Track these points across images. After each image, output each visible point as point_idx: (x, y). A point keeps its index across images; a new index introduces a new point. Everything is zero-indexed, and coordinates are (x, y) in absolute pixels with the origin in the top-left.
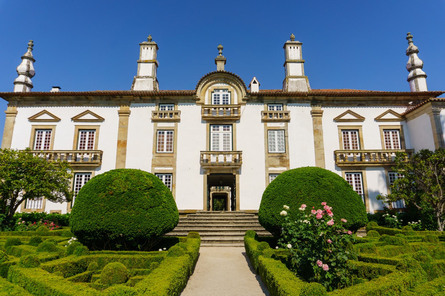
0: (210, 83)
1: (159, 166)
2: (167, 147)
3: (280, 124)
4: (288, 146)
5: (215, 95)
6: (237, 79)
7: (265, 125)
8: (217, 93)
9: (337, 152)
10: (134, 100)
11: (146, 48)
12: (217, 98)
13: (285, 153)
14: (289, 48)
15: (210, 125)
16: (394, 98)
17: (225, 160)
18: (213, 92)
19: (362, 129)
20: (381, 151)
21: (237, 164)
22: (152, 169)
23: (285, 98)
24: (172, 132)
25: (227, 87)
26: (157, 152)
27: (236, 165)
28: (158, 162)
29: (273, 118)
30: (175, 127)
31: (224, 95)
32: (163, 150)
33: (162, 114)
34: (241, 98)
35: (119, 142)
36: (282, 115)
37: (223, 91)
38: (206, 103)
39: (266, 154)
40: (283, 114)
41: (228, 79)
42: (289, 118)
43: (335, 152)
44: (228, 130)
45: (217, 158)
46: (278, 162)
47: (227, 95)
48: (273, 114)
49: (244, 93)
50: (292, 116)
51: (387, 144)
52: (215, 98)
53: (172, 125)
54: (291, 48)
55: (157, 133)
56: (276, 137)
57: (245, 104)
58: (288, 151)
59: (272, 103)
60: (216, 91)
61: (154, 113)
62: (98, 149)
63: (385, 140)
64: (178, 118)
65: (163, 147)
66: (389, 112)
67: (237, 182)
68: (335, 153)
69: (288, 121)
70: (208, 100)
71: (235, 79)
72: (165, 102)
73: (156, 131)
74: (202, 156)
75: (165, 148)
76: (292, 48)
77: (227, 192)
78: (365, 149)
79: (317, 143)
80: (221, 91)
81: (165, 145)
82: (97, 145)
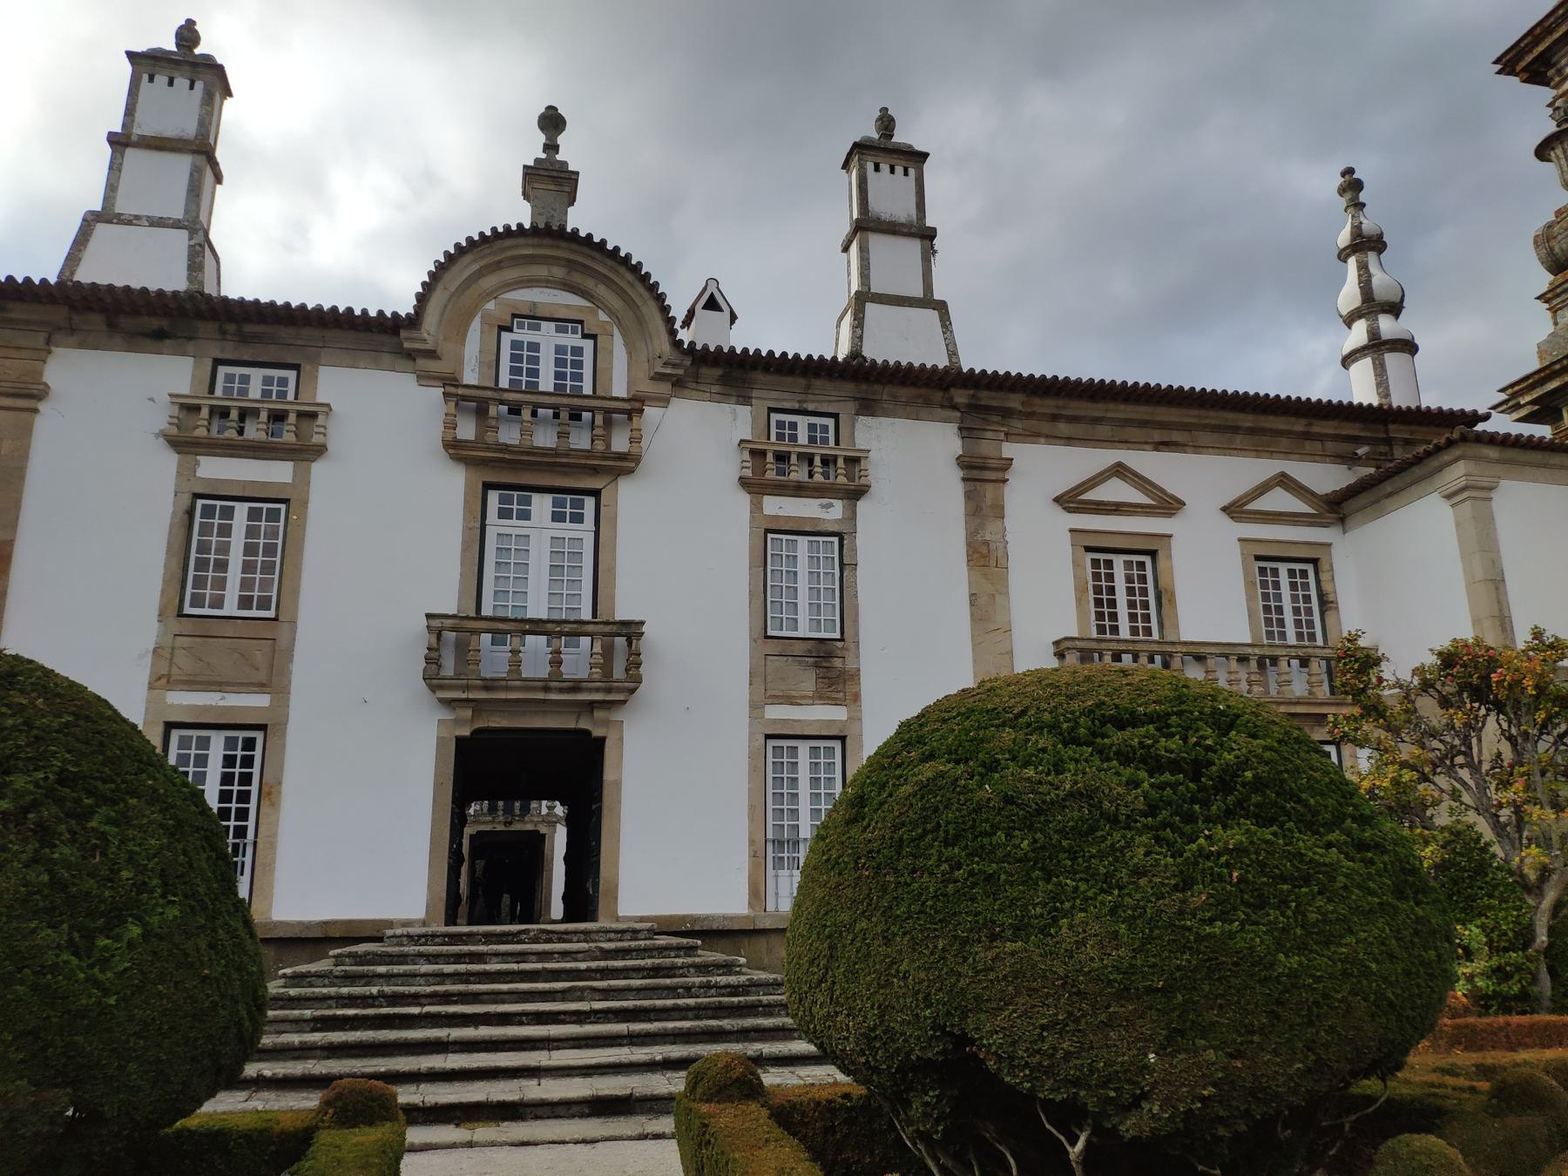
0: (489, 282)
1: (192, 684)
2: (246, 584)
5: (516, 345)
6: (629, 276)
7: (757, 507)
9: (1063, 646)
12: (525, 357)
13: (842, 640)
14: (870, 166)
15: (487, 486)
16: (1299, 426)
17: (556, 662)
18: (510, 329)
19: (1170, 549)
20: (1250, 650)
22: (148, 702)
23: (848, 388)
25: (580, 309)
26: (188, 610)
27: (609, 690)
28: (184, 663)
29: (793, 476)
30: (292, 485)
31: (560, 350)
32: (218, 602)
33: (224, 413)
36: (832, 466)
37: (558, 330)
38: (470, 377)
39: (753, 640)
40: (835, 462)
41: (586, 269)
42: (863, 482)
43: (1057, 643)
45: (515, 652)
46: (807, 681)
47: (578, 351)
48: (794, 459)
49: (663, 345)
50: (878, 472)
51: (1268, 622)
52: (515, 358)
53: (278, 472)
54: (877, 169)
55: (190, 513)
56: (803, 567)
57: (664, 401)
58: (857, 634)
59: (787, 405)
60: (521, 326)
61: (183, 406)
63: (1261, 603)
64: (317, 439)
65: (221, 584)
66: (1278, 484)
67: (609, 775)
69: (855, 494)
71: (617, 272)
73: (186, 500)
74: (434, 640)
76: (885, 168)
78: (1183, 639)
81: (234, 574)
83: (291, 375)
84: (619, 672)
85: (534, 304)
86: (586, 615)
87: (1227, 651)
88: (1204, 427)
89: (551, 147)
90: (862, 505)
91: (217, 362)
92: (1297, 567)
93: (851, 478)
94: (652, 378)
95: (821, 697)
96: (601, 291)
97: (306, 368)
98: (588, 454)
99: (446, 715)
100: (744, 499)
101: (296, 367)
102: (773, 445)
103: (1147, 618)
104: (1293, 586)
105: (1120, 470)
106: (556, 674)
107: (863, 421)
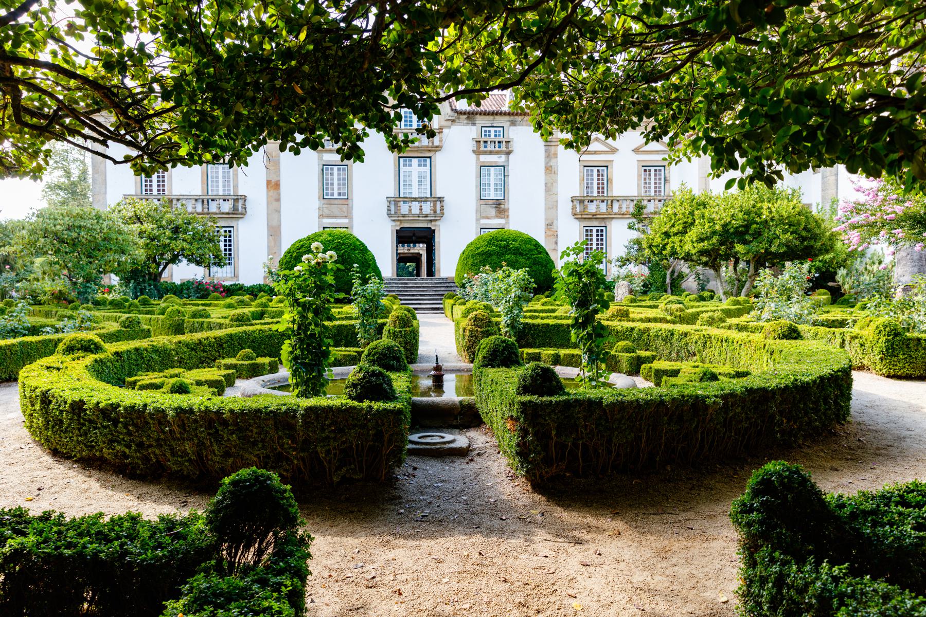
1: (329, 217)
2: (339, 189)
7: (478, 159)
17: (421, 209)
21: (438, 215)
23: (507, 118)
28: (326, 212)
29: (489, 149)
32: (332, 195)
35: (269, 182)
46: (493, 212)
57: (449, 127)
62: (240, 194)
67: (437, 240)
75: (336, 192)
77: (421, 252)
79: (549, 185)
82: (236, 187)
84: (438, 211)
86: (429, 196)
87: (626, 199)
90: (511, 156)
92: (658, 168)
93: (507, 148)
95: (497, 217)
98: (427, 147)
99: (394, 224)
100: (474, 156)
102: (484, 138)
103: (603, 188)
104: (655, 175)
106: (421, 213)
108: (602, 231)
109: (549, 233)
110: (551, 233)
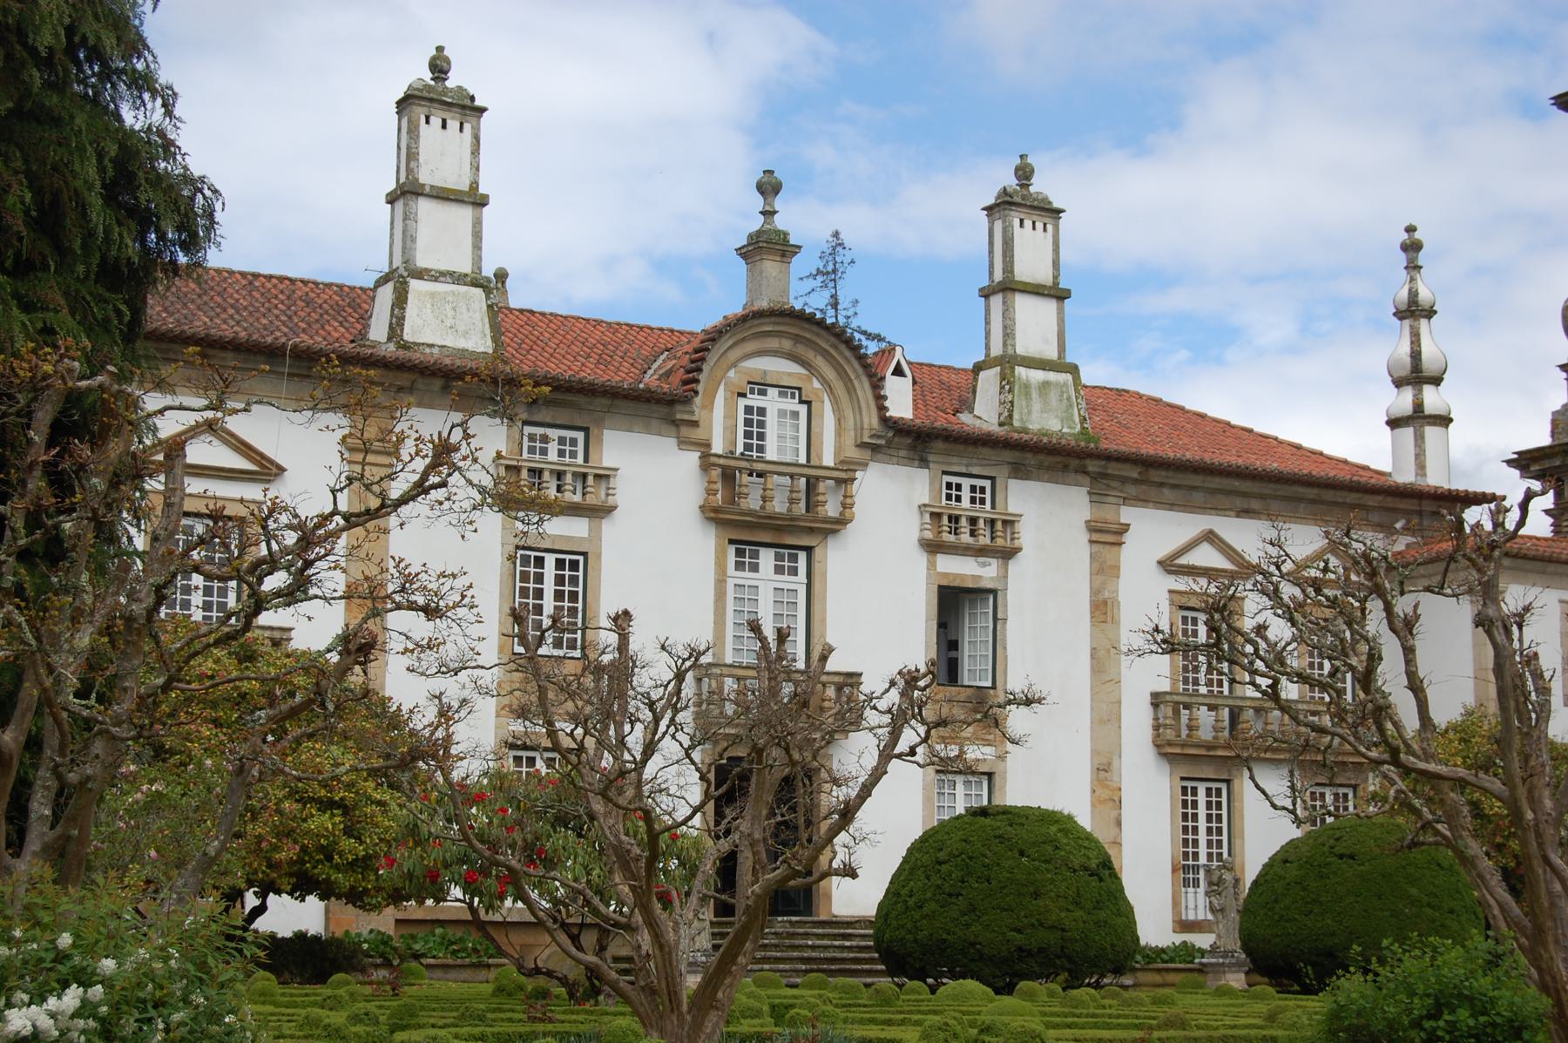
0: (734, 354)
3: (984, 565)
4: (1006, 658)
5: (748, 410)
6: (848, 353)
7: (932, 565)
8: (755, 401)
10: (411, 390)
11: (436, 121)
14: (1016, 222)
18: (743, 395)
23: (1008, 455)
24: (578, 561)
30: (590, 539)
34: (849, 439)
37: (781, 394)
44: (793, 571)
49: (871, 420)
52: (748, 423)
60: (752, 392)
68: (1157, 700)
69: (1008, 554)
70: (725, 428)
71: (836, 348)
72: (544, 415)
73: (512, 548)
76: (1028, 223)
80: (773, 393)
83: (580, 436)
85: (765, 372)
88: (1276, 498)
89: (768, 214)
90: (1013, 565)
91: (525, 423)
94: (858, 446)
96: (819, 362)
97: (594, 431)
100: (922, 558)
101: (586, 430)
105: (1210, 537)
107: (1012, 483)
108: (1219, 791)
109: (1105, 794)
110: (1105, 794)
